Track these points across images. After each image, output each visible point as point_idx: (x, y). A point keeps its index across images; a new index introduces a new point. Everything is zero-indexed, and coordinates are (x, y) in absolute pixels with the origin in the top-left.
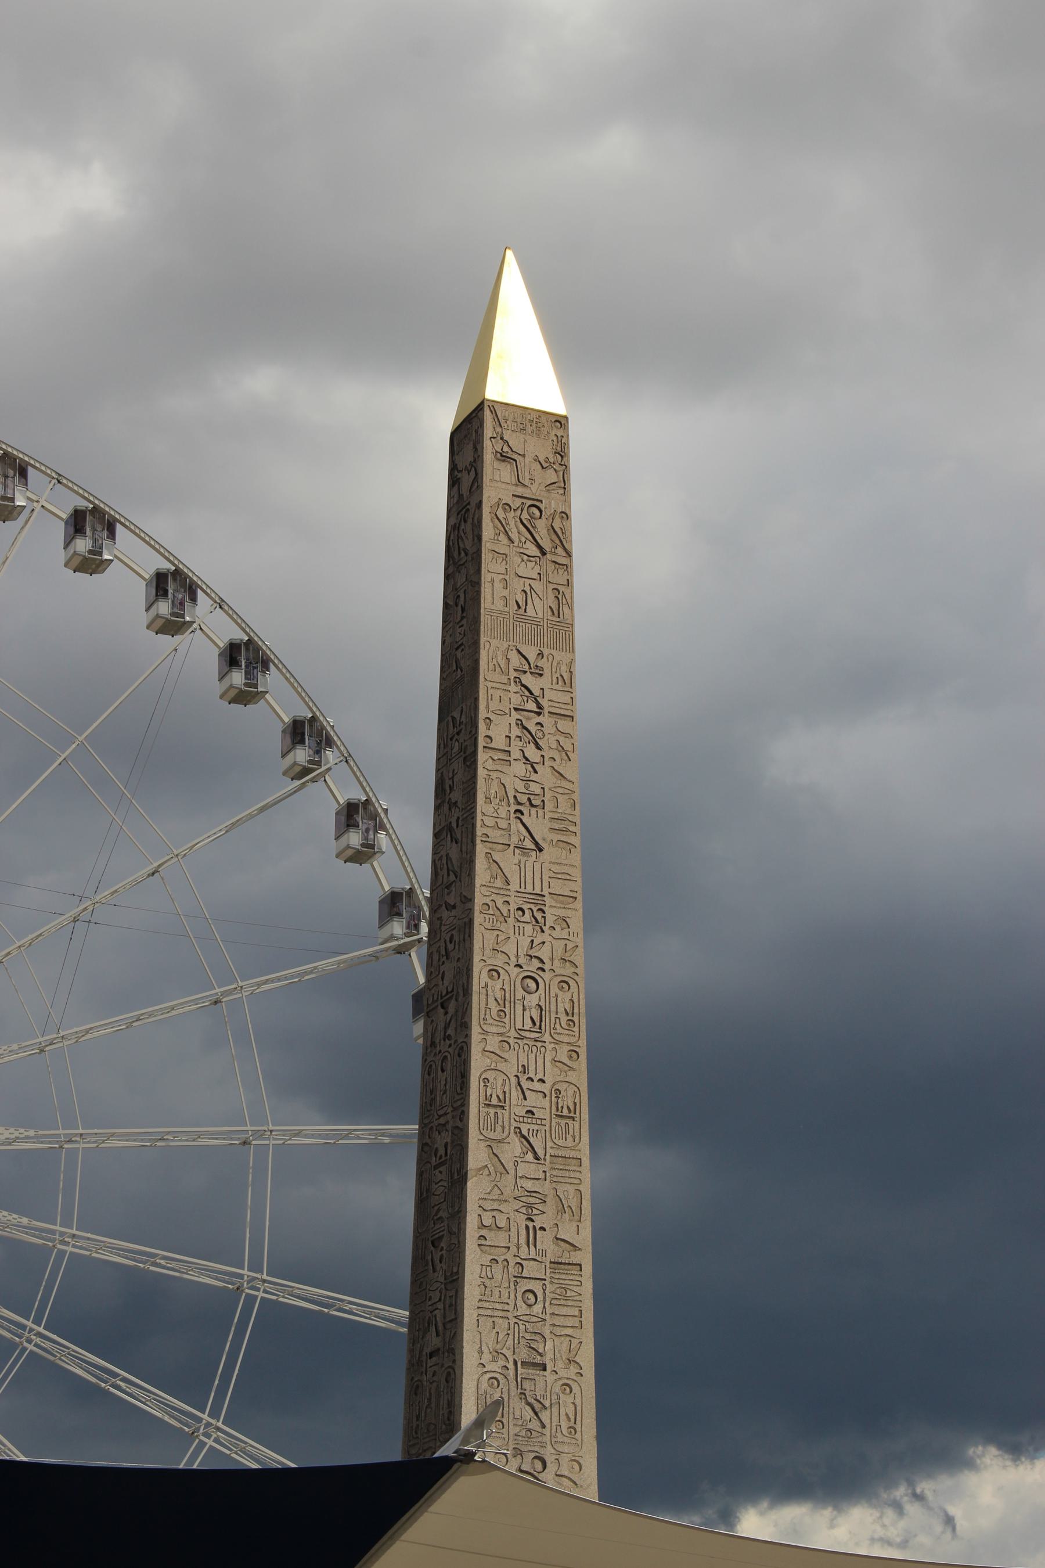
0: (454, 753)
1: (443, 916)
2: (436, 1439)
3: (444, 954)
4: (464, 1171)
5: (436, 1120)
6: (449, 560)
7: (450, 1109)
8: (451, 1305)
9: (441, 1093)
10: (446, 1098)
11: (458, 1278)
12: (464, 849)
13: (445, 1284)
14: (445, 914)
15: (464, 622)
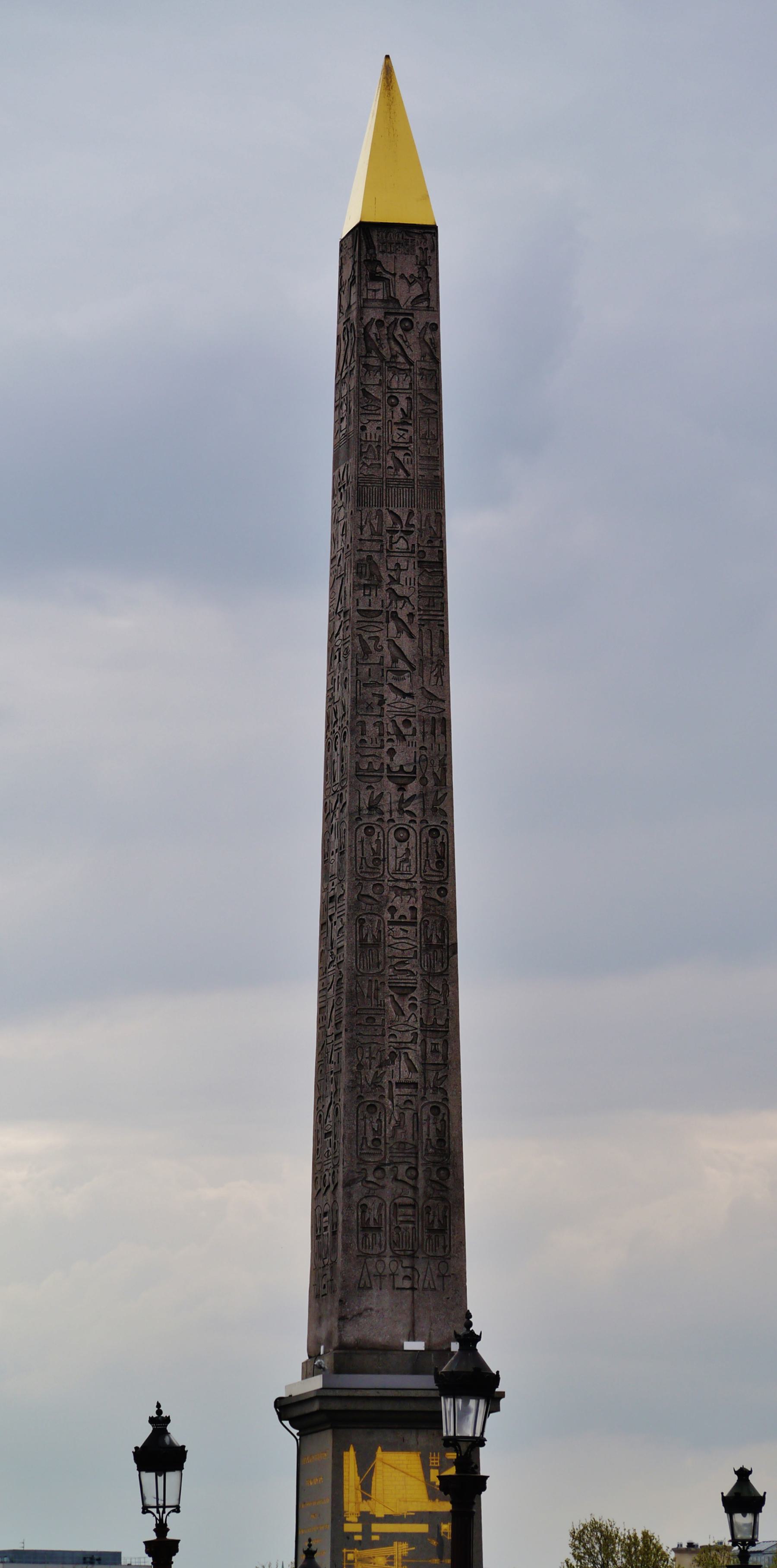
0: (398, 549)
1: (386, 696)
2: (417, 1158)
3: (391, 730)
4: (451, 942)
5: (388, 881)
6: (369, 351)
7: (418, 879)
8: (435, 1051)
9: (398, 862)
10: (409, 866)
11: (448, 1031)
12: (426, 648)
13: (421, 1030)
14: (391, 697)
15: (410, 429)
